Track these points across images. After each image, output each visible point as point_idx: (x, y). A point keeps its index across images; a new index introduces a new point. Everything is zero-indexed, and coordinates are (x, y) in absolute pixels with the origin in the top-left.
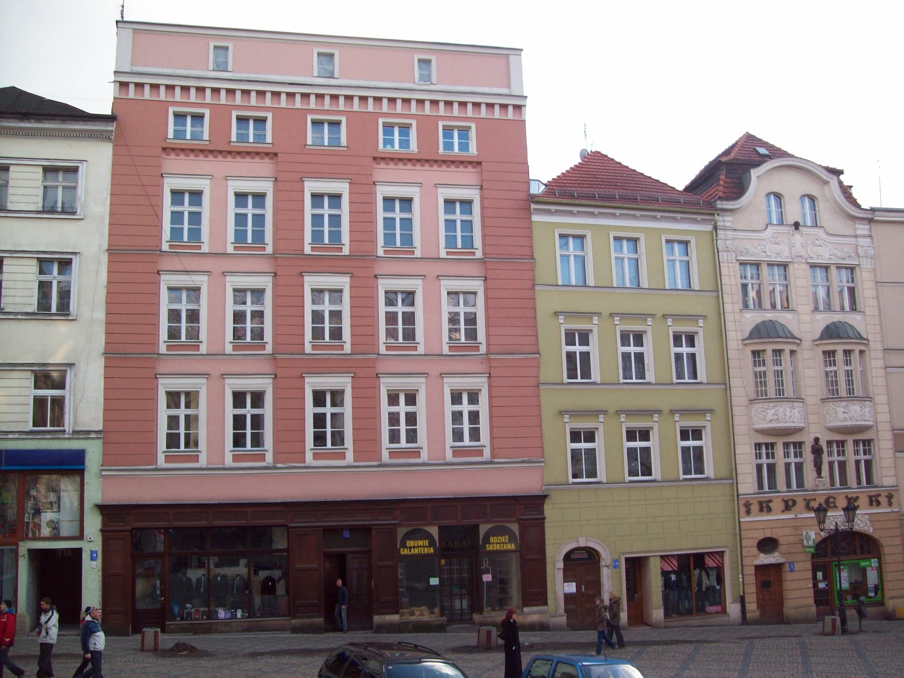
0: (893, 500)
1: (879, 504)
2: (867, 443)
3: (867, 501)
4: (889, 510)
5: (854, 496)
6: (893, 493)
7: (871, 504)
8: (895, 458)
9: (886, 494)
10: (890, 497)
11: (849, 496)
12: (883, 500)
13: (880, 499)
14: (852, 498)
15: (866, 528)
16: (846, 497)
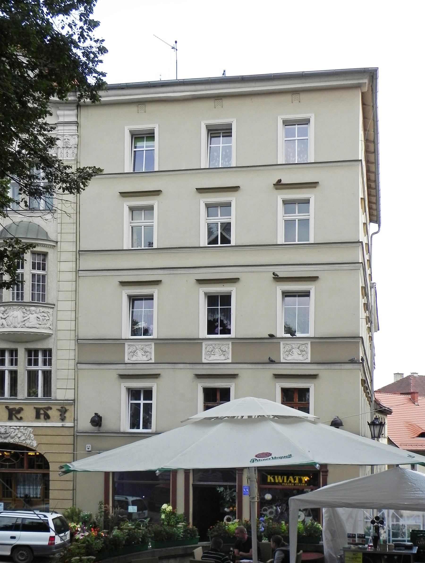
0: (67, 415)
1: (47, 417)
2: (48, 352)
3: (33, 413)
4: (60, 424)
5: (17, 407)
6: (67, 407)
7: (38, 417)
8: (77, 370)
9: (59, 407)
10: (63, 412)
11: (11, 407)
12: (54, 413)
13: (50, 412)
14: (14, 409)
15: (28, 442)
16: (7, 407)
